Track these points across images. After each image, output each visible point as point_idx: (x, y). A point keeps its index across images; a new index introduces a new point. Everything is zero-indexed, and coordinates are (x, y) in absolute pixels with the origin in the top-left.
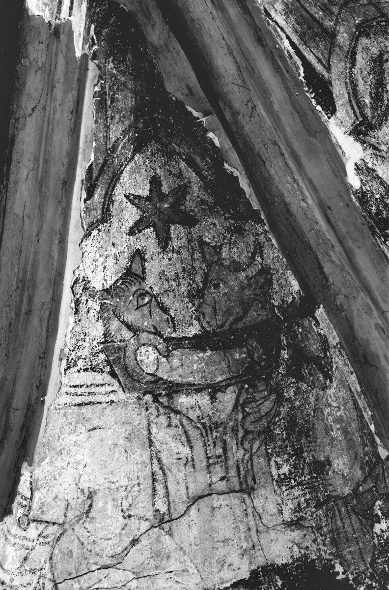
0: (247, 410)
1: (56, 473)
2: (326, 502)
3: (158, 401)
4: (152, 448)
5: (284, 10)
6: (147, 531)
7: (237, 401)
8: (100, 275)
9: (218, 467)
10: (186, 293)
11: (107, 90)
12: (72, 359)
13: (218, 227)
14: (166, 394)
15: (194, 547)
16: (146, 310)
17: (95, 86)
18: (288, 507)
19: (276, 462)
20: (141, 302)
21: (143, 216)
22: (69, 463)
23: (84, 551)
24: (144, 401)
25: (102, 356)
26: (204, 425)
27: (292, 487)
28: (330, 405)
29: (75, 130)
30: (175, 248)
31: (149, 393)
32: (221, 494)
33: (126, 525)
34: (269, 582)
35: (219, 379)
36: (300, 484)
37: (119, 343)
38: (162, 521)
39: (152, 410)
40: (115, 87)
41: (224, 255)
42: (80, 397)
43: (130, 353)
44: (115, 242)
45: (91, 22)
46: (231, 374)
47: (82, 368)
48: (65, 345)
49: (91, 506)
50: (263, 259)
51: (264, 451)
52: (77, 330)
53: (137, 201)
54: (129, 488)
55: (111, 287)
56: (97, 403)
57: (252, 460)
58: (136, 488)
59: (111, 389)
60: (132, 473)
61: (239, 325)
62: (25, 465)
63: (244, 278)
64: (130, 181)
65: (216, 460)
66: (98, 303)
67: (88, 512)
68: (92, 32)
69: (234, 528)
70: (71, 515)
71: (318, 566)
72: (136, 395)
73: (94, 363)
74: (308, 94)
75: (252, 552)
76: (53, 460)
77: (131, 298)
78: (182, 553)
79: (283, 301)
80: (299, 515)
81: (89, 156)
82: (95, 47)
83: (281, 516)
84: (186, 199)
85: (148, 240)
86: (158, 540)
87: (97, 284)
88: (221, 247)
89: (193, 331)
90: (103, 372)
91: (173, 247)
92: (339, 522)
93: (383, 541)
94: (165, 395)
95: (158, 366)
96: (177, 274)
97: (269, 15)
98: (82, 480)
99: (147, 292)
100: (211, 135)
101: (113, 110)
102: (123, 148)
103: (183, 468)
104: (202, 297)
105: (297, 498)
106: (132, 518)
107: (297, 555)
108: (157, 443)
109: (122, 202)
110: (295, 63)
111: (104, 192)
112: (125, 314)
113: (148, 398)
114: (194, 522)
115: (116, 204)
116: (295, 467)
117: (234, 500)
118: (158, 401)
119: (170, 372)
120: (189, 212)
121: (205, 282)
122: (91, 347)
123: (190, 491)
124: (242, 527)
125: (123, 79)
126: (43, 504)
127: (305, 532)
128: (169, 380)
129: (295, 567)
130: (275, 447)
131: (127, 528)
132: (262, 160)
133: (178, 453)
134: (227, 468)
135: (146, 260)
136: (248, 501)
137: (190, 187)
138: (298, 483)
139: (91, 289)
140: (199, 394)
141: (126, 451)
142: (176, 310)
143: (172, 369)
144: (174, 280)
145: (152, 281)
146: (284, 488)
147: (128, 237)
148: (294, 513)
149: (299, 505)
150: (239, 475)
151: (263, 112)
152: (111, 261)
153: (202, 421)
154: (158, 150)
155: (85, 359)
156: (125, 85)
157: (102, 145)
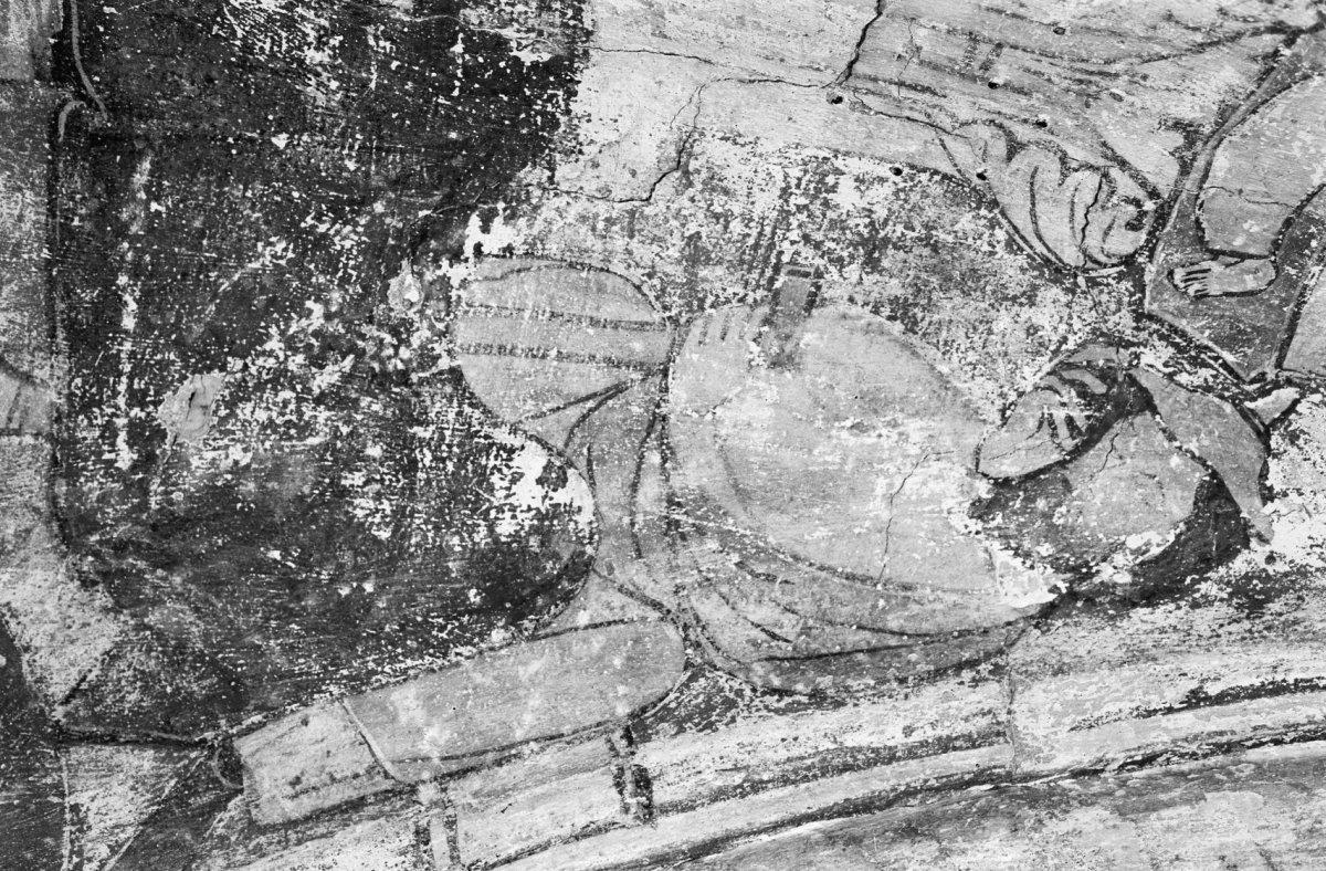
7: (1123, 164)
9: (959, 54)
18: (733, 161)
19: (882, 180)
27: (785, 193)
32: (865, 30)
34: (540, 33)
36: (785, 215)
46: (1213, 191)
51: (932, 165)
71: (532, 175)
75: (648, 28)
80: (697, 180)
83: (720, 135)
92: (609, 311)
93: (492, 463)
107: (585, 130)
127: (641, 177)
129: (553, 115)
130: (924, 195)
140: (1215, 108)
149: (726, 192)
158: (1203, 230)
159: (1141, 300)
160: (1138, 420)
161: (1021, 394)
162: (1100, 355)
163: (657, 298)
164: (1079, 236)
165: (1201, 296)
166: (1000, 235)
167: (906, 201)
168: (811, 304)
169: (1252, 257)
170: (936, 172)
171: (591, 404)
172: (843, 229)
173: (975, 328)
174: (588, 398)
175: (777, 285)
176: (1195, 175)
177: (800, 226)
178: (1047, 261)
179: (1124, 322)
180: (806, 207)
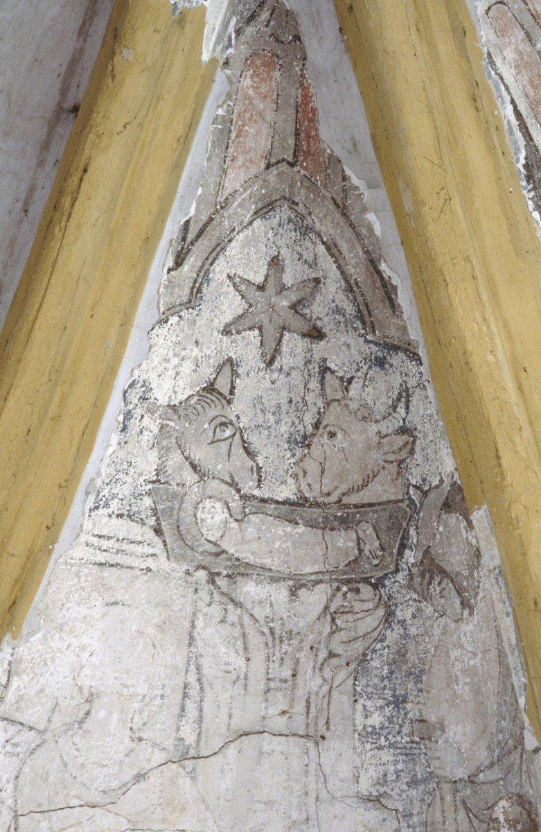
0: (339, 622)
1: (48, 656)
2: (425, 781)
3: (213, 582)
4: (192, 648)
5: (515, 61)
6: (160, 766)
7: (326, 608)
8: (168, 384)
9: (279, 695)
10: (286, 436)
11: (234, 117)
12: (104, 496)
13: (353, 351)
14: (228, 576)
15: (222, 802)
16: (224, 447)
17: (219, 106)
19: (364, 706)
20: (219, 435)
21: (247, 310)
22: (69, 646)
23: (66, 776)
24: (194, 578)
25: (148, 502)
26: (272, 631)
27: (380, 748)
28: (462, 647)
29: (178, 167)
30: (284, 367)
31: (204, 568)
33: (132, 751)
35: (308, 570)
36: (392, 746)
37: (175, 487)
38: (185, 756)
39: (204, 594)
40: (247, 115)
41: (352, 393)
42: (105, 553)
43: (188, 505)
44: (201, 340)
45: (233, 13)
46: (327, 566)
47: (116, 512)
48: (99, 474)
49: (88, 713)
50: (407, 413)
51: (351, 687)
52: (121, 457)
53: (243, 287)
54: (147, 699)
55: (181, 403)
56: (127, 567)
57: (330, 696)
58: (158, 701)
59: (151, 551)
60: (157, 678)
61: (354, 499)
62: (8, 637)
63: (374, 433)
64: (240, 256)
65: (279, 684)
66: (157, 423)
67: (81, 722)
68: (231, 29)
69: (285, 788)
70: (57, 721)
72: (185, 567)
73: (135, 509)
74: (525, 192)
76: (48, 636)
77: (206, 426)
78: (203, 807)
79: (424, 480)
80: (382, 790)
81: (189, 208)
82: (231, 51)
83: (356, 785)
84: (314, 299)
85: (247, 348)
86: (173, 782)
87: (162, 396)
88: (350, 381)
89: (286, 492)
90: (144, 524)
91: (281, 366)
92: (438, 815)
94: (226, 576)
95: (225, 532)
96: (279, 406)
97: (492, 63)
98: (83, 674)
99: (231, 423)
100: (371, 217)
101: (236, 148)
102: (240, 205)
103: (230, 687)
104: (309, 446)
105: (384, 764)
106: (144, 742)
108: (199, 643)
109: (222, 284)
110: (515, 142)
111: (200, 264)
112: (193, 447)
113: (202, 575)
114: (230, 767)
115: (213, 284)
116: (390, 720)
117: (294, 747)
118: (213, 582)
119: (240, 544)
120: (315, 320)
121: (316, 426)
122: (135, 485)
123: (234, 721)
124: (297, 788)
125: (261, 106)
126: (21, 697)
127: (385, 816)
128: (236, 556)
130: (368, 685)
131: (133, 755)
132: (445, 280)
133: (228, 664)
134: (293, 700)
135: (238, 376)
136: (313, 753)
137: (324, 284)
138: (390, 744)
139: (152, 400)
140: (275, 585)
141: (154, 645)
142: (267, 457)
143: (243, 541)
144: (273, 414)
145: (241, 409)
146: (368, 746)
147: (220, 336)
148: (375, 785)
149: (385, 775)
150: (308, 713)
151: (459, 210)
152: (187, 367)
153: (271, 625)
154: (290, 220)
155: (122, 500)
156: (261, 115)
157: (211, 194)
158: (349, 562)
159: (391, 573)
160: (433, 553)
161: (435, 611)
162: (418, 580)
163: (432, 795)
164: (370, 612)
165: (383, 549)
166: (379, 646)
167: (372, 693)
168: (423, 721)
169: (358, 536)
170: (354, 684)
171: (471, 815)
172: (392, 717)
173: (418, 642)
174: (469, 817)
175: (418, 739)
176: (320, 577)
177: (394, 737)
178: (386, 620)
179: (401, 577)
180: (385, 737)
